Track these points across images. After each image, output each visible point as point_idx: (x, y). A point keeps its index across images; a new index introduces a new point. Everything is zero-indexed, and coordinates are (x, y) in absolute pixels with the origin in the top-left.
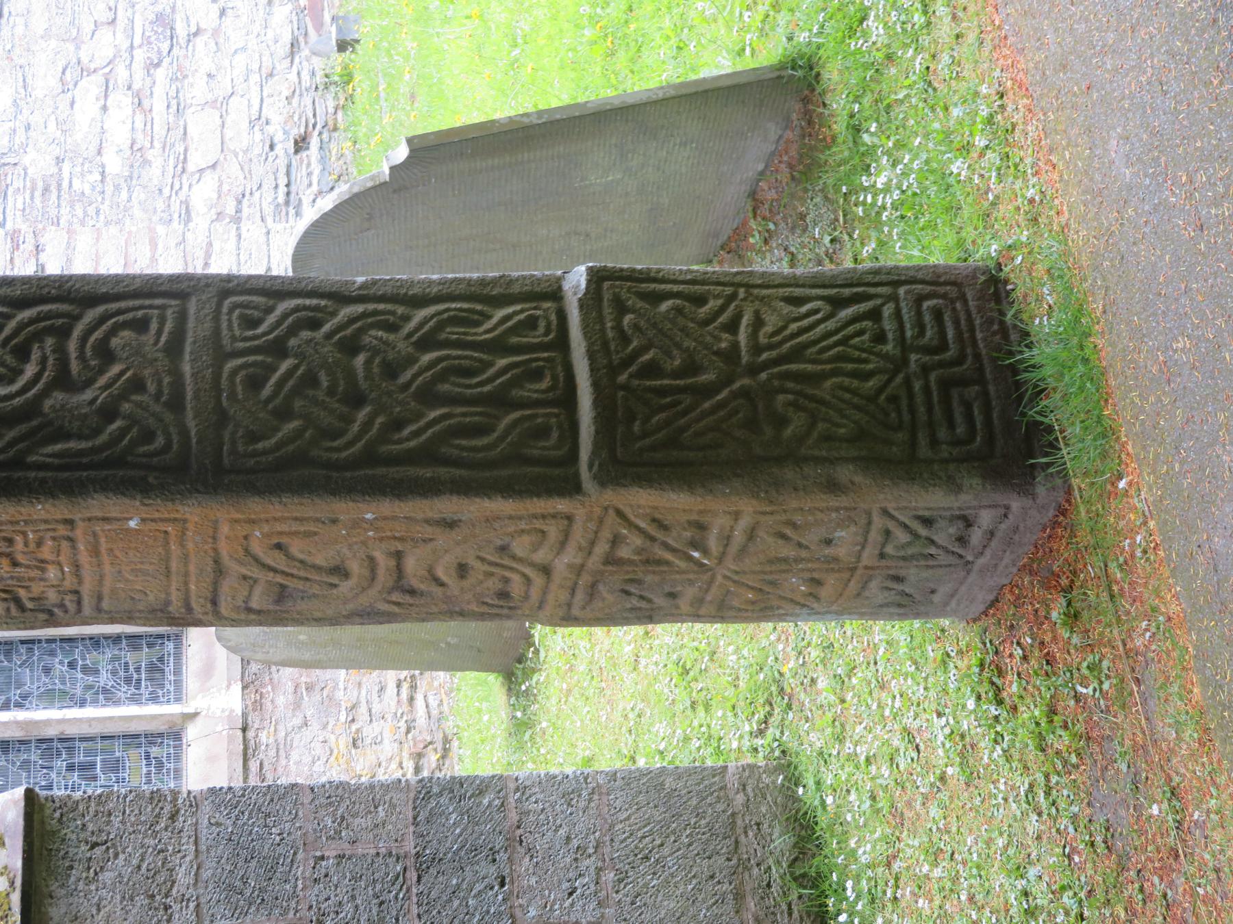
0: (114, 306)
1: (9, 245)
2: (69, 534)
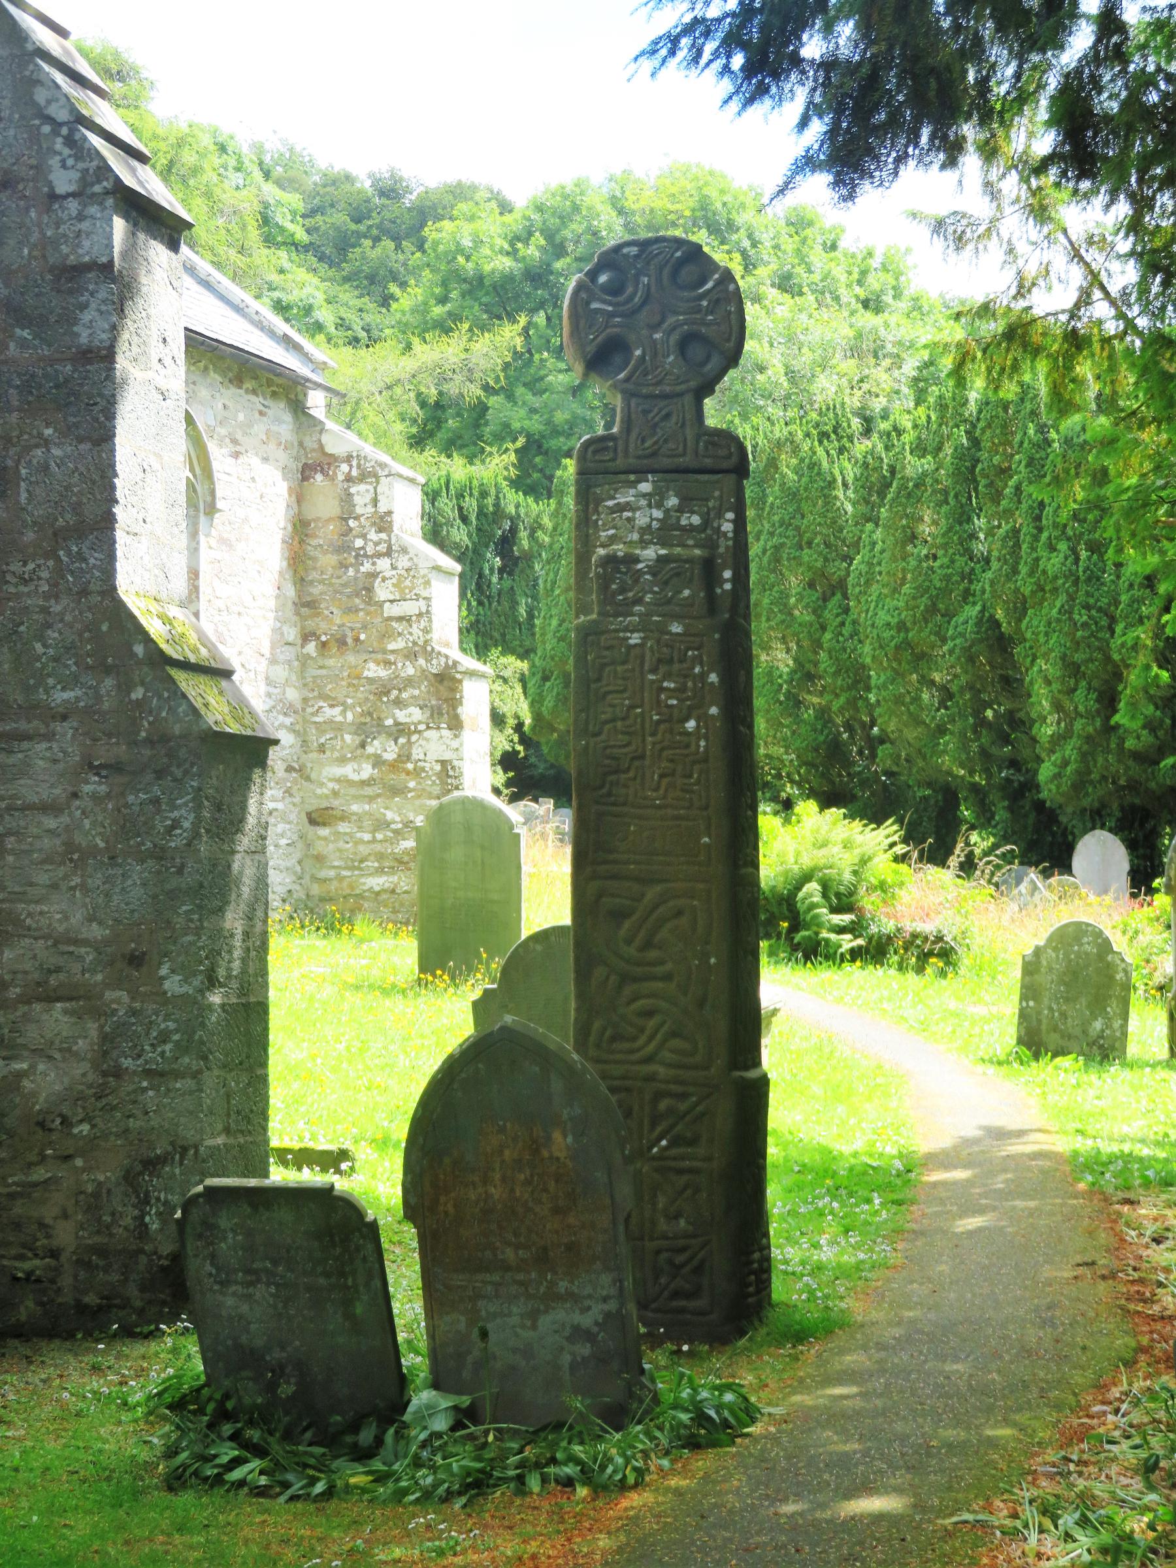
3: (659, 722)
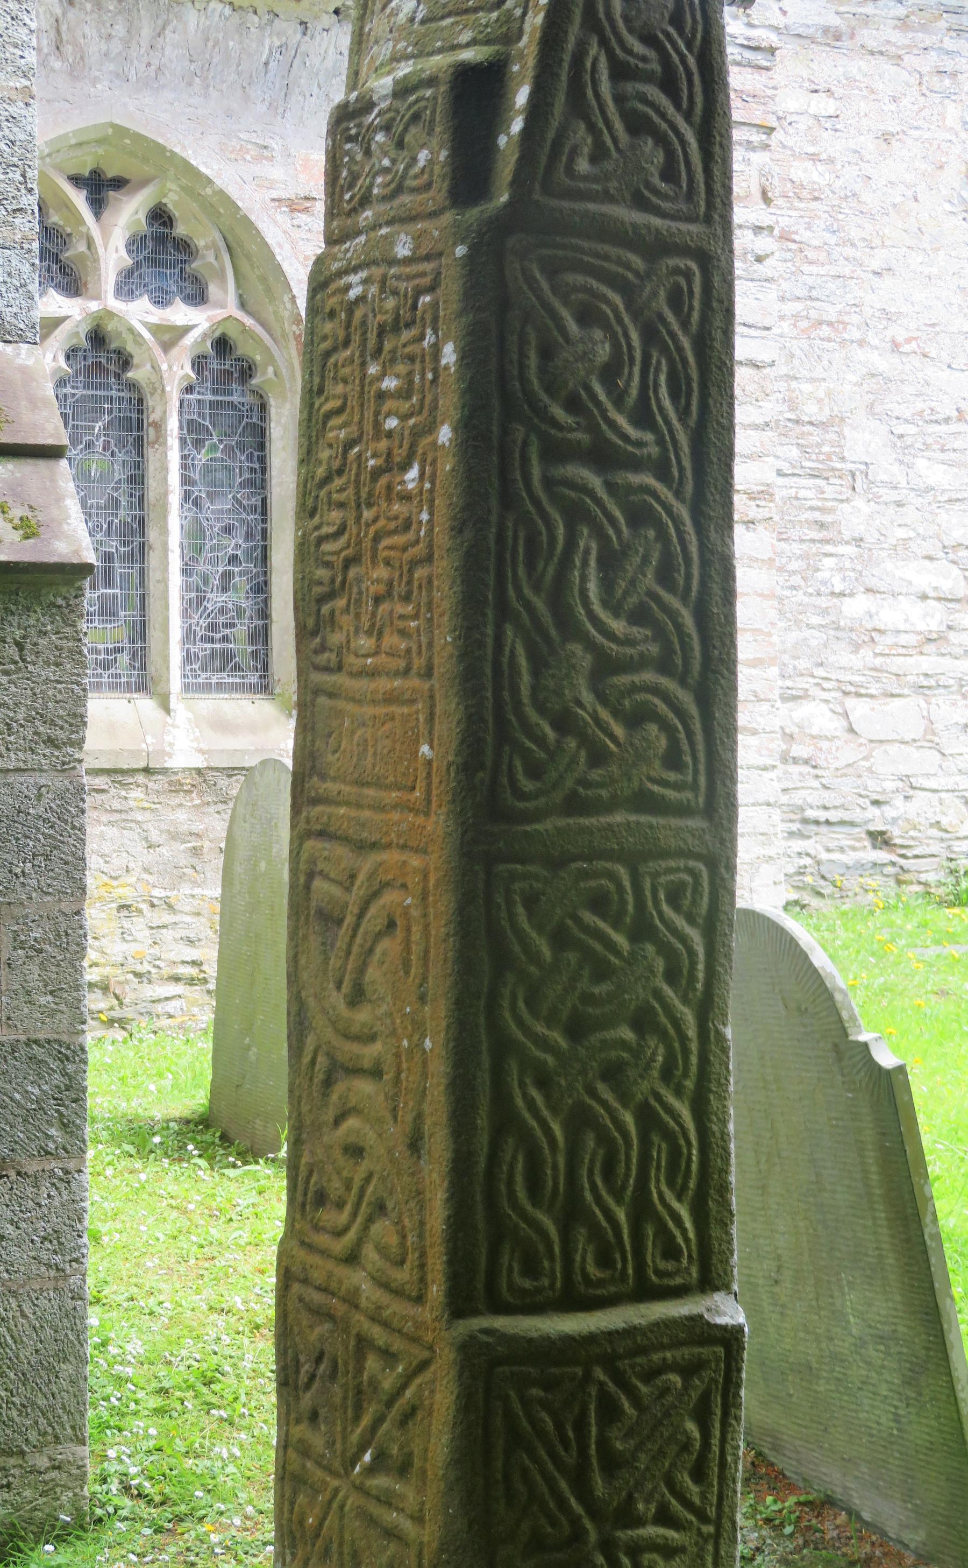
0: (697, 726)
1: (756, 488)
2: (414, 671)
3: (376, 474)
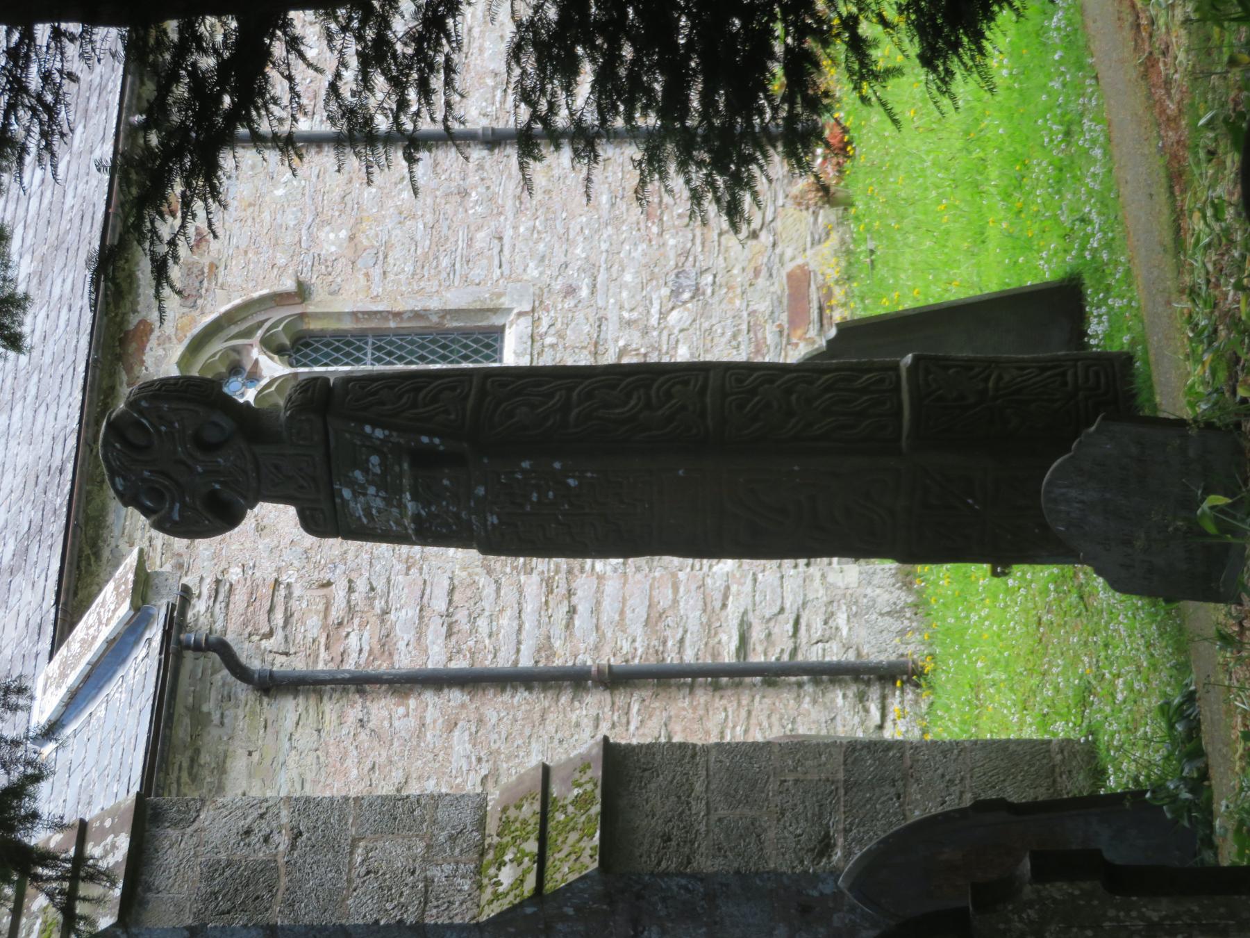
1: (544, 589)
